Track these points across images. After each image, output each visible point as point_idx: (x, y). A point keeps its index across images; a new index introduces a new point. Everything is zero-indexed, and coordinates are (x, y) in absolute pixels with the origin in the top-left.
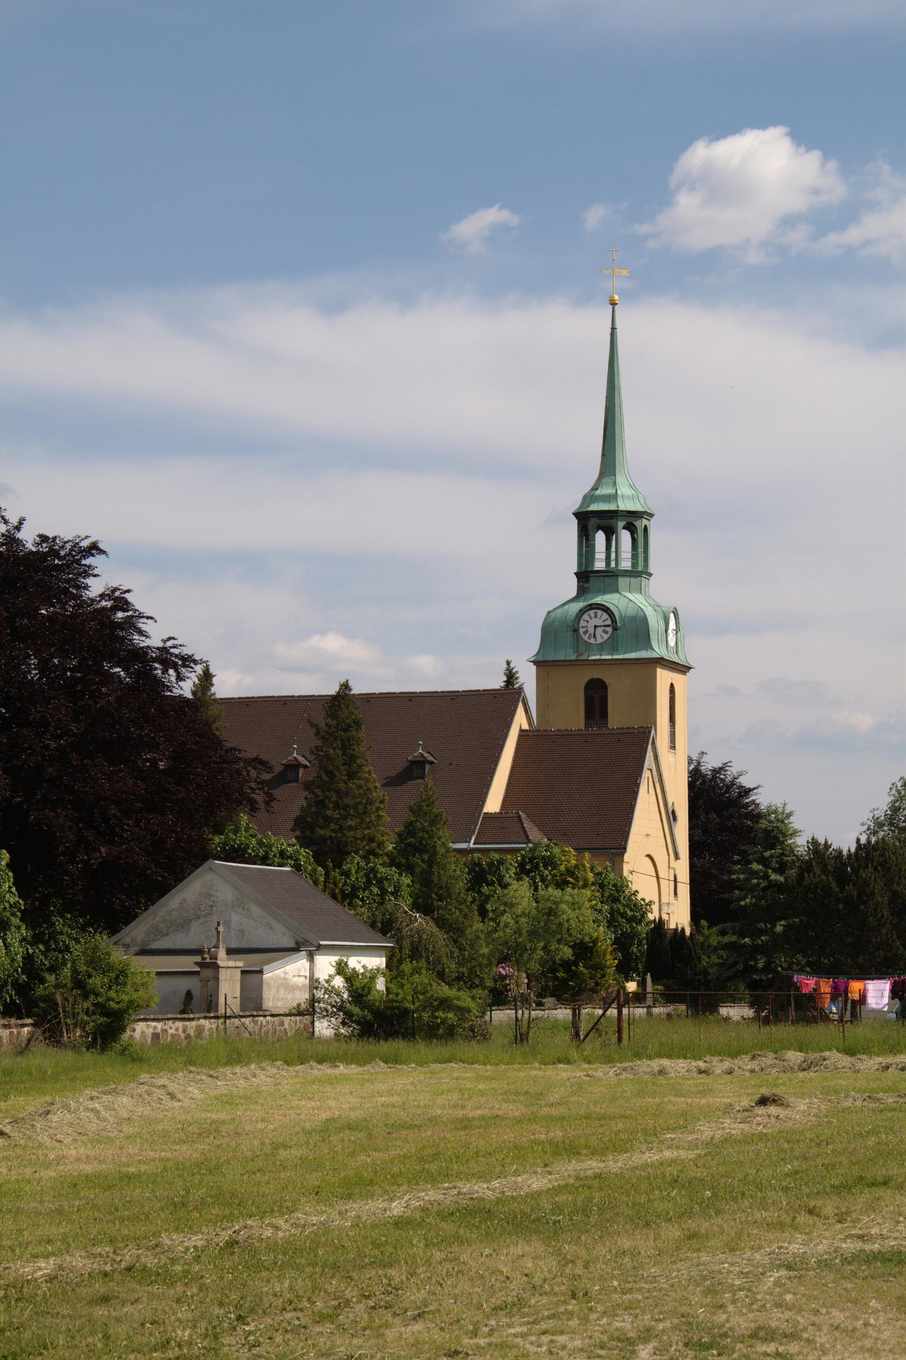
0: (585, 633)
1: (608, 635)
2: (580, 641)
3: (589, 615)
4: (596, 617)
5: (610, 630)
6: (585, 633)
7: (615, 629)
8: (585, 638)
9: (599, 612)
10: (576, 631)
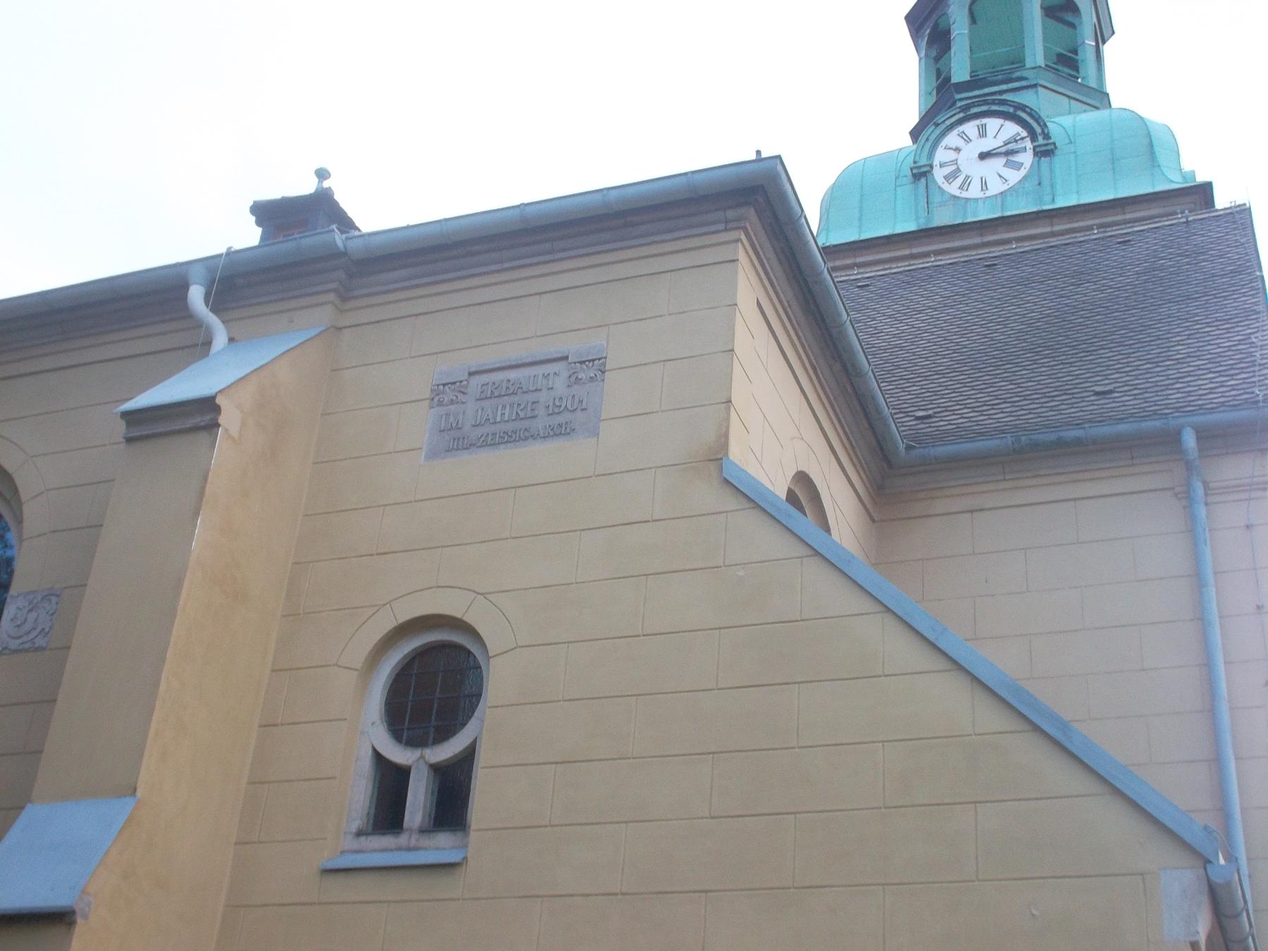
0: (950, 178)
1: (1023, 172)
2: (936, 198)
3: (963, 136)
4: (983, 133)
5: (1027, 158)
6: (950, 178)
7: (1045, 152)
8: (953, 189)
9: (993, 124)
10: (921, 174)
